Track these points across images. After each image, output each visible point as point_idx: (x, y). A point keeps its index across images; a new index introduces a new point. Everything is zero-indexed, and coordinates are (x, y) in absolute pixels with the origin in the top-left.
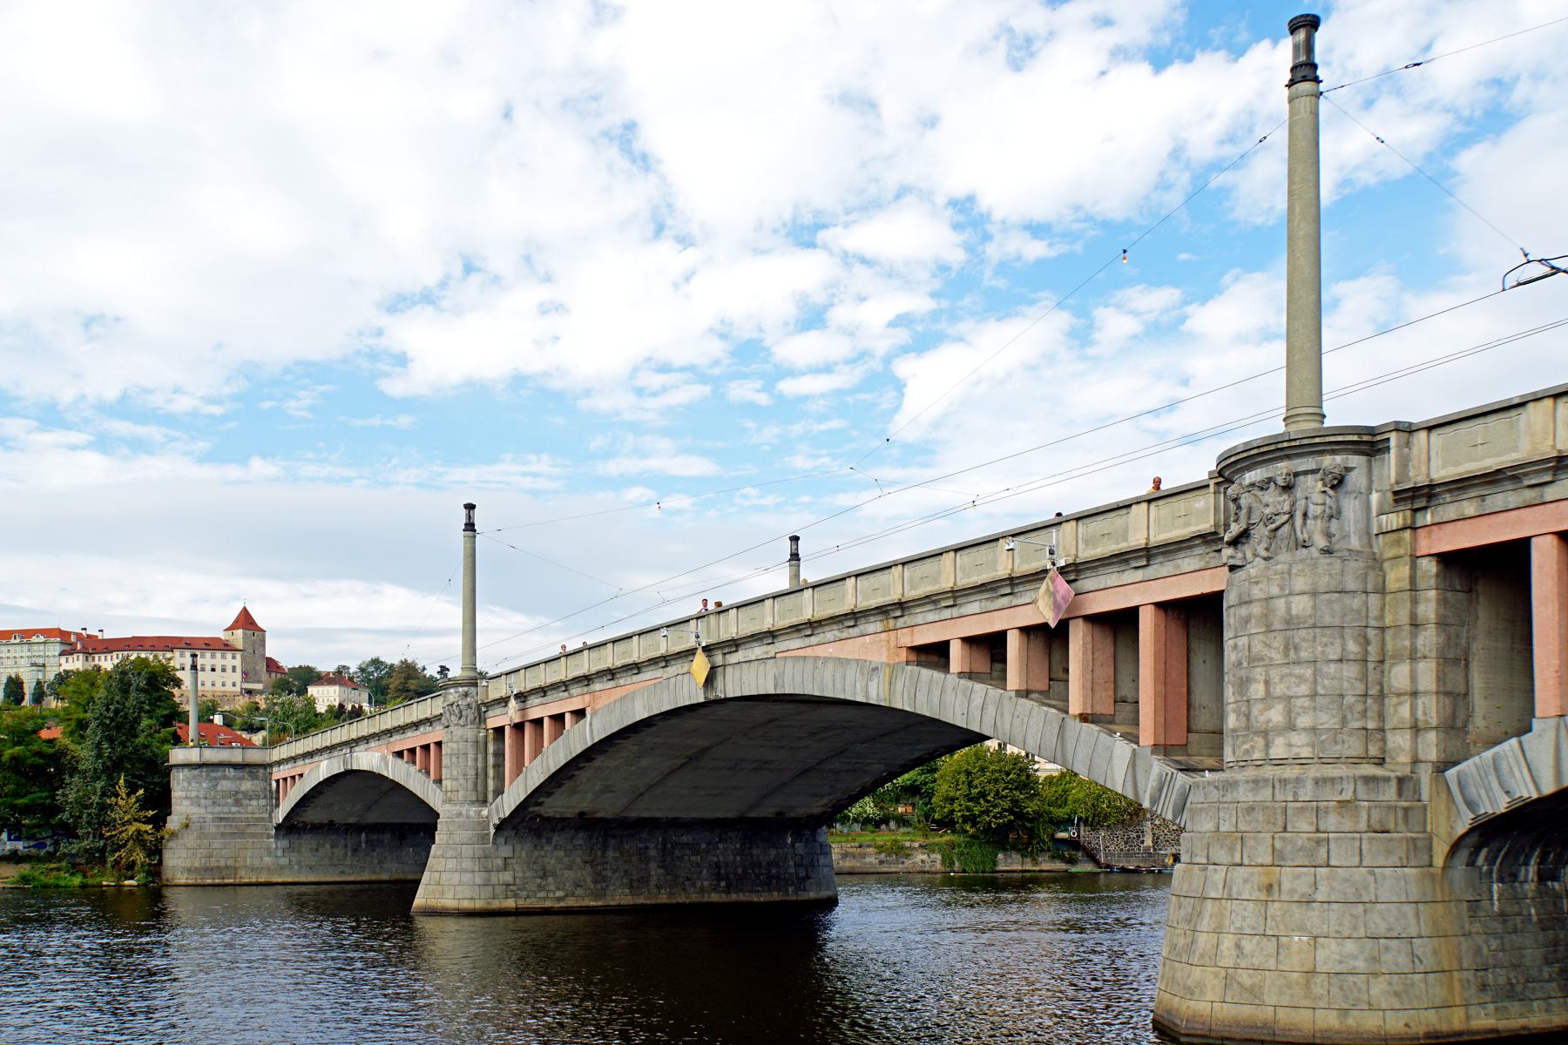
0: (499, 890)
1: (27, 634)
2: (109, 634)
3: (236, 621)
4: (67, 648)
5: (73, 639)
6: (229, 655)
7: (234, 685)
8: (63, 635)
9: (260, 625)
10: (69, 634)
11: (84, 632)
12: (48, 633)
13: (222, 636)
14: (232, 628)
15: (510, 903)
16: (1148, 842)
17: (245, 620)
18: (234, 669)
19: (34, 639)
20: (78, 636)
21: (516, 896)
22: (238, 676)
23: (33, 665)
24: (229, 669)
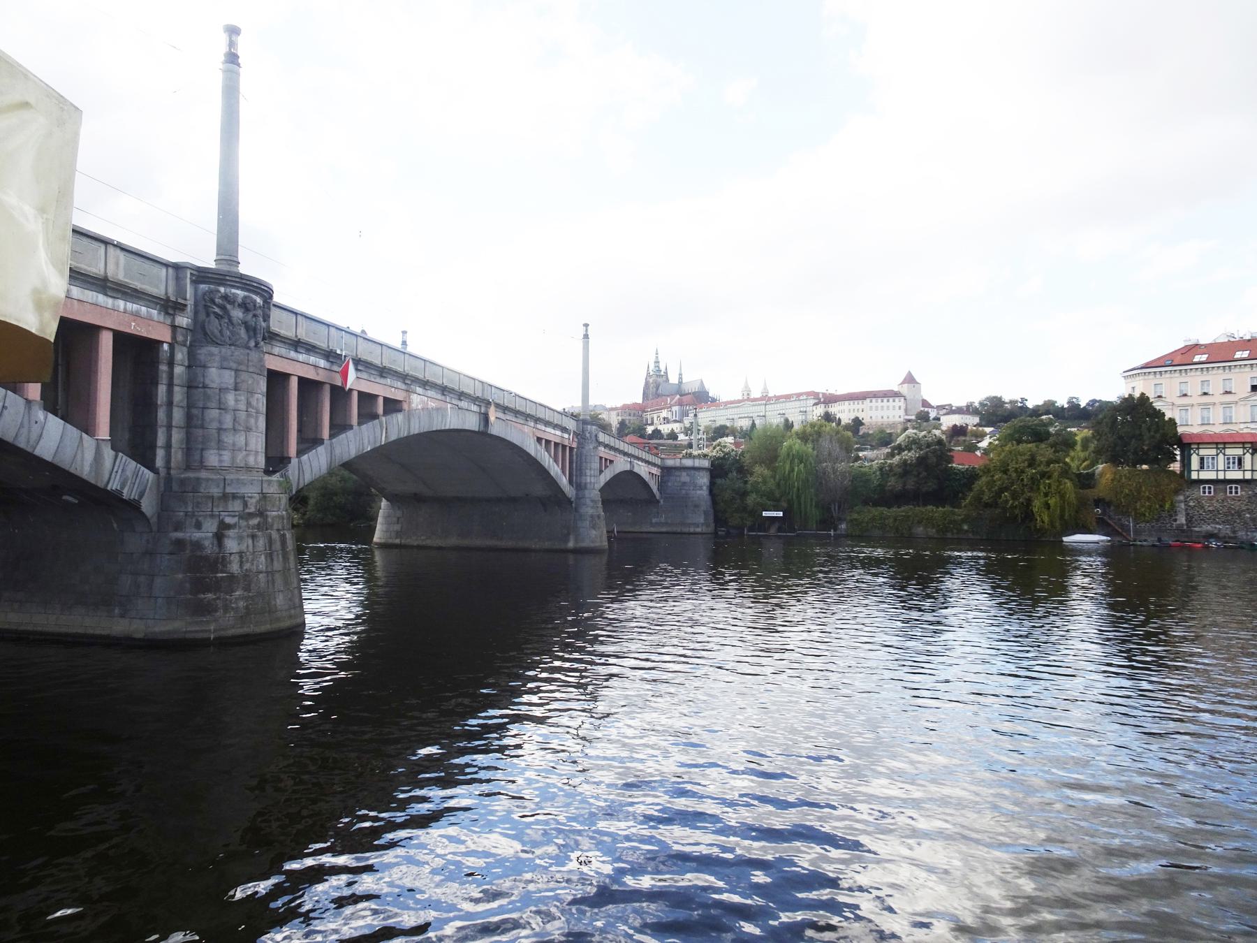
0: (393, 534)
1: (799, 395)
2: (839, 393)
3: (905, 379)
4: (816, 401)
5: (821, 396)
6: (897, 399)
7: (900, 417)
8: (815, 395)
9: (918, 380)
10: (818, 394)
11: (828, 393)
12: (808, 394)
13: (896, 389)
14: (903, 383)
15: (397, 541)
16: (1182, 519)
17: (910, 379)
18: (900, 408)
19: (801, 398)
20: (824, 394)
21: (401, 538)
22: (902, 412)
23: (801, 412)
24: (897, 408)
